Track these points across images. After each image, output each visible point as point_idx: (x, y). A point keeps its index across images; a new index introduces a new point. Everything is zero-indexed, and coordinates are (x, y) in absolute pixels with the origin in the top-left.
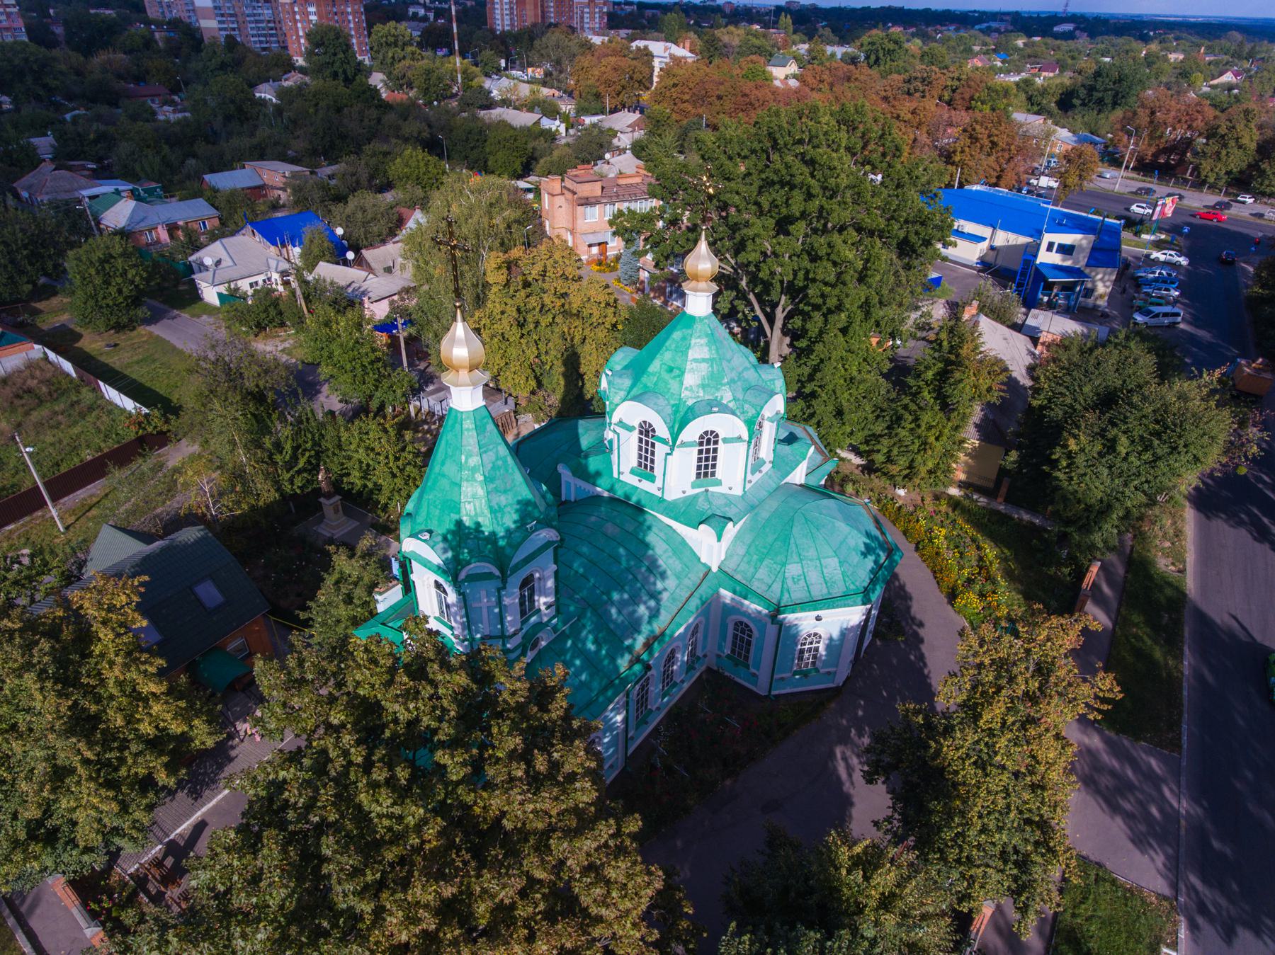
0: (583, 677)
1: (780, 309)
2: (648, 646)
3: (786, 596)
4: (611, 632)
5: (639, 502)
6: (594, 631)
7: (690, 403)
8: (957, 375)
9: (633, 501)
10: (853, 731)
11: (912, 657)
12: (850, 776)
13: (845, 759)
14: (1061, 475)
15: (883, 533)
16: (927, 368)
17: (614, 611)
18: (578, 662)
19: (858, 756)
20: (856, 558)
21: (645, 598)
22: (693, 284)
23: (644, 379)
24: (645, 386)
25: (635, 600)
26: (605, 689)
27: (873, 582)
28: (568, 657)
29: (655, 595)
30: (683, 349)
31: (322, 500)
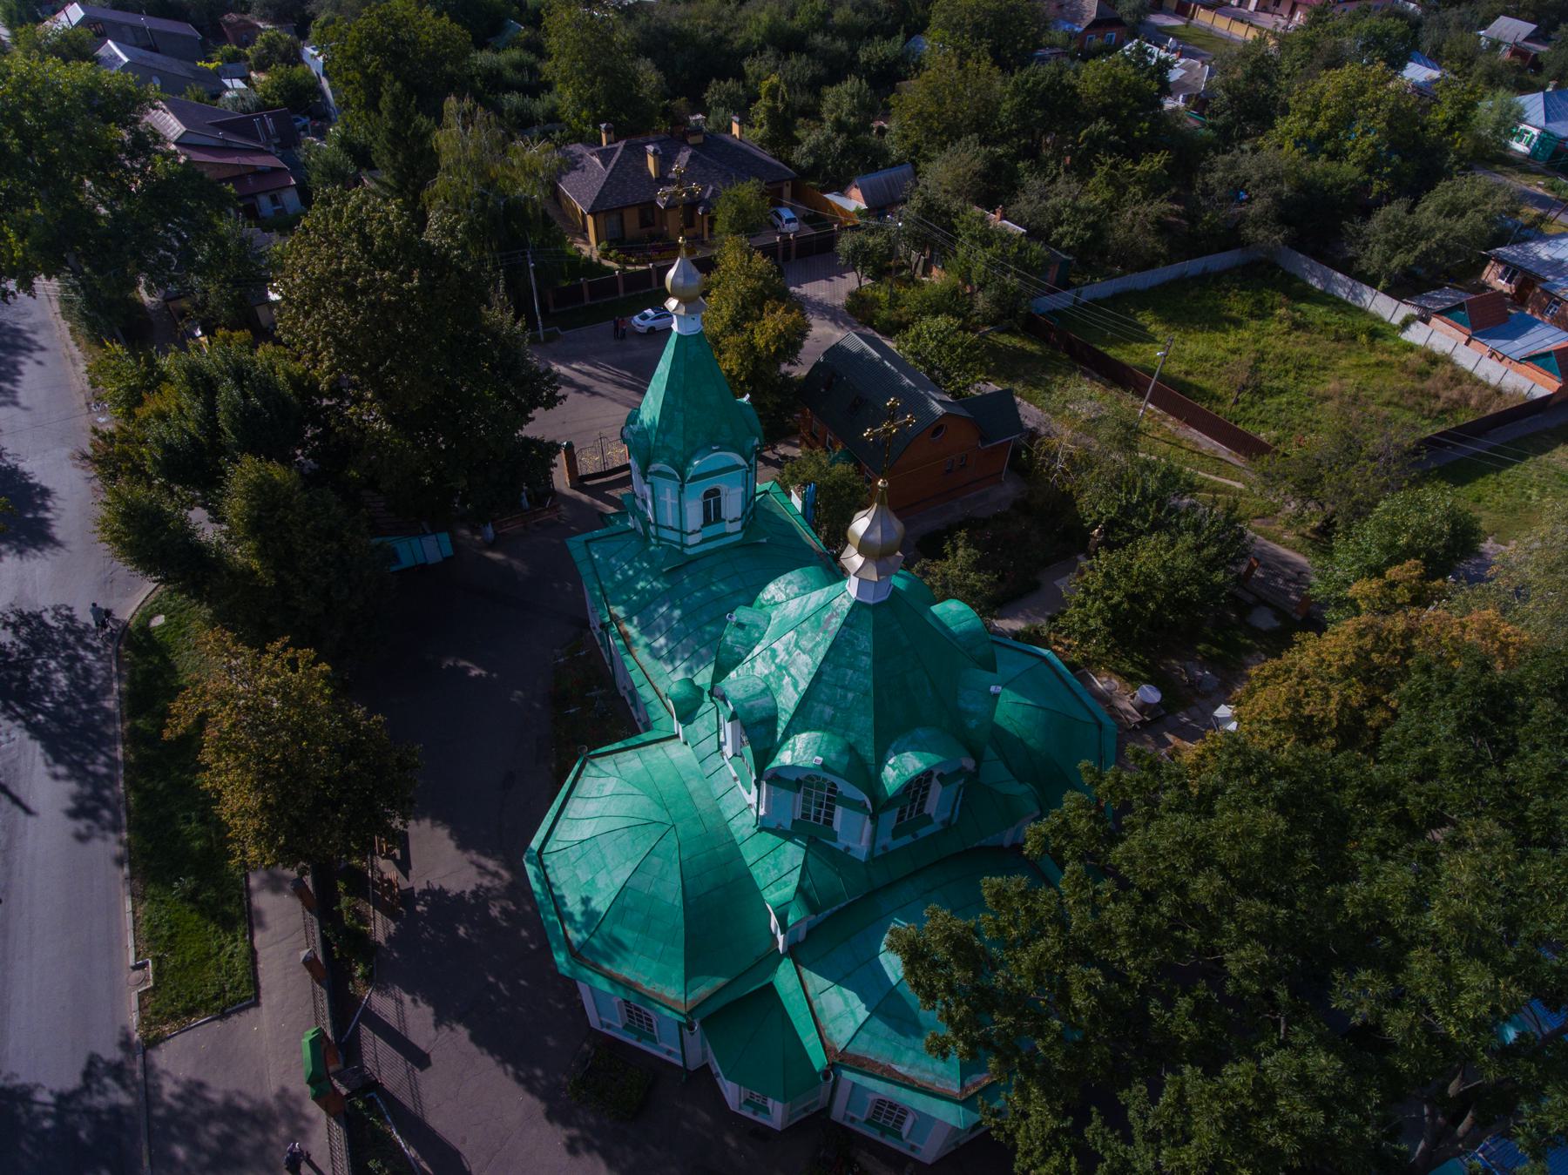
0: (620, 577)
2: (624, 636)
4: (649, 603)
6: (653, 591)
10: (513, 908)
11: (539, 1072)
12: (480, 866)
13: (496, 875)
15: (613, 979)
17: (664, 609)
18: (631, 573)
19: (488, 889)
20: (584, 876)
21: (671, 646)
25: (671, 634)
26: (602, 589)
27: (547, 884)
28: (637, 564)
29: (671, 658)
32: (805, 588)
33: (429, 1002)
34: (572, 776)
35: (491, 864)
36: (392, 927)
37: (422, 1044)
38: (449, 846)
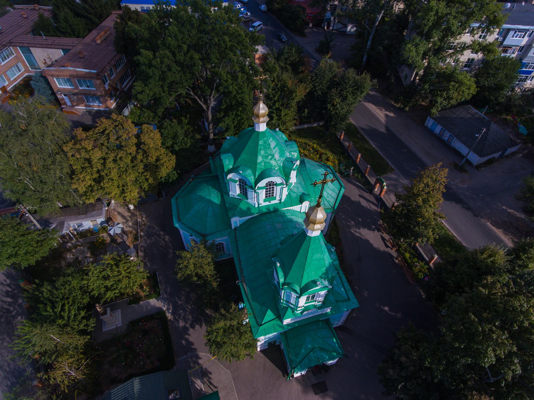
1: (212, 97)
3: (330, 203)
5: (274, 208)
7: (282, 165)
8: (294, 95)
9: (272, 209)
12: (361, 235)
13: (356, 232)
14: (333, 113)
16: (274, 97)
19: (357, 228)
22: (261, 119)
23: (258, 166)
24: (260, 168)
30: (267, 146)
31: (102, 317)
32: (271, 171)
33: (363, 206)
34: (337, 205)
35: (357, 234)
36: (379, 223)
37: (361, 198)
38: (371, 241)
